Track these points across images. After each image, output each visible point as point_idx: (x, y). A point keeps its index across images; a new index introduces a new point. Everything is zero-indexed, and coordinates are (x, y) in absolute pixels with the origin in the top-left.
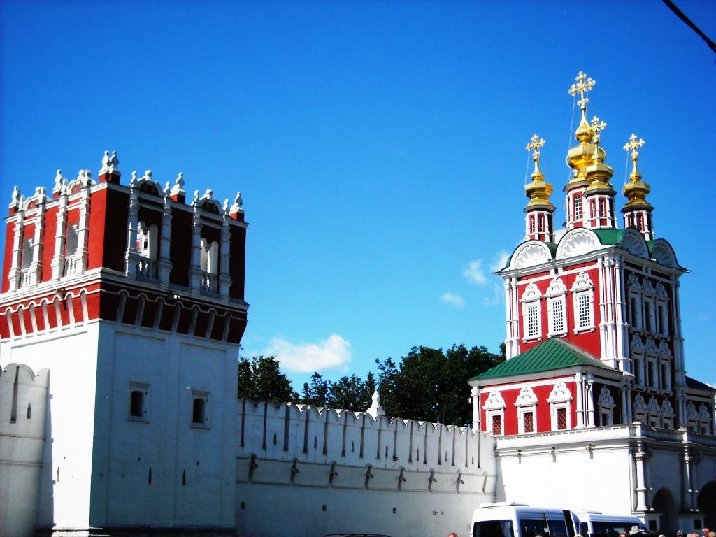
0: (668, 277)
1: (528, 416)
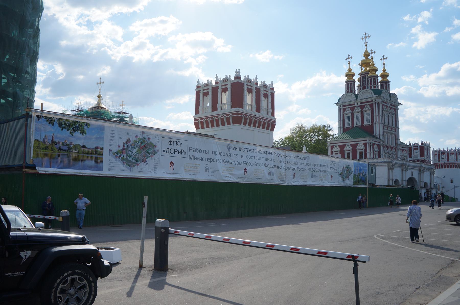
0: (395, 106)
1: (348, 154)
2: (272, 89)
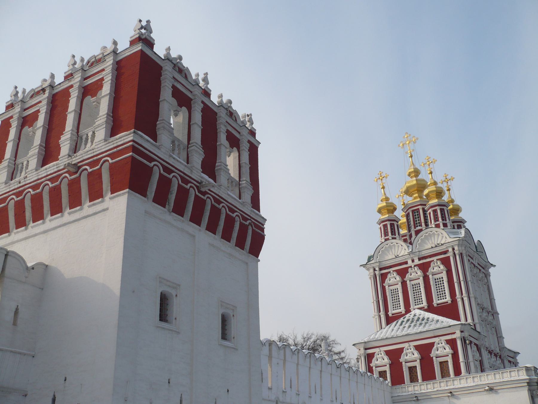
0: (483, 268)
1: (412, 370)
2: (253, 133)
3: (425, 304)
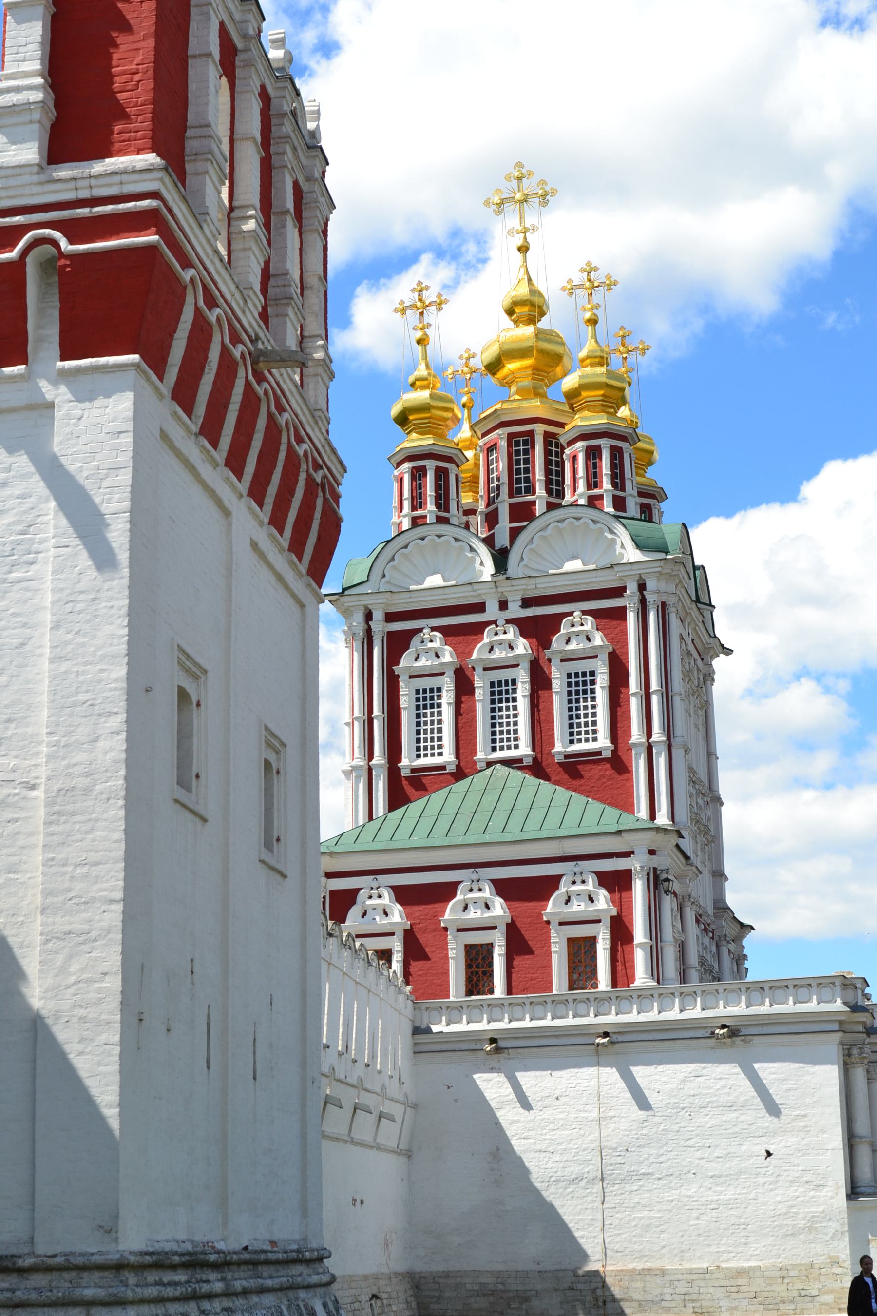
3: (524, 749)
